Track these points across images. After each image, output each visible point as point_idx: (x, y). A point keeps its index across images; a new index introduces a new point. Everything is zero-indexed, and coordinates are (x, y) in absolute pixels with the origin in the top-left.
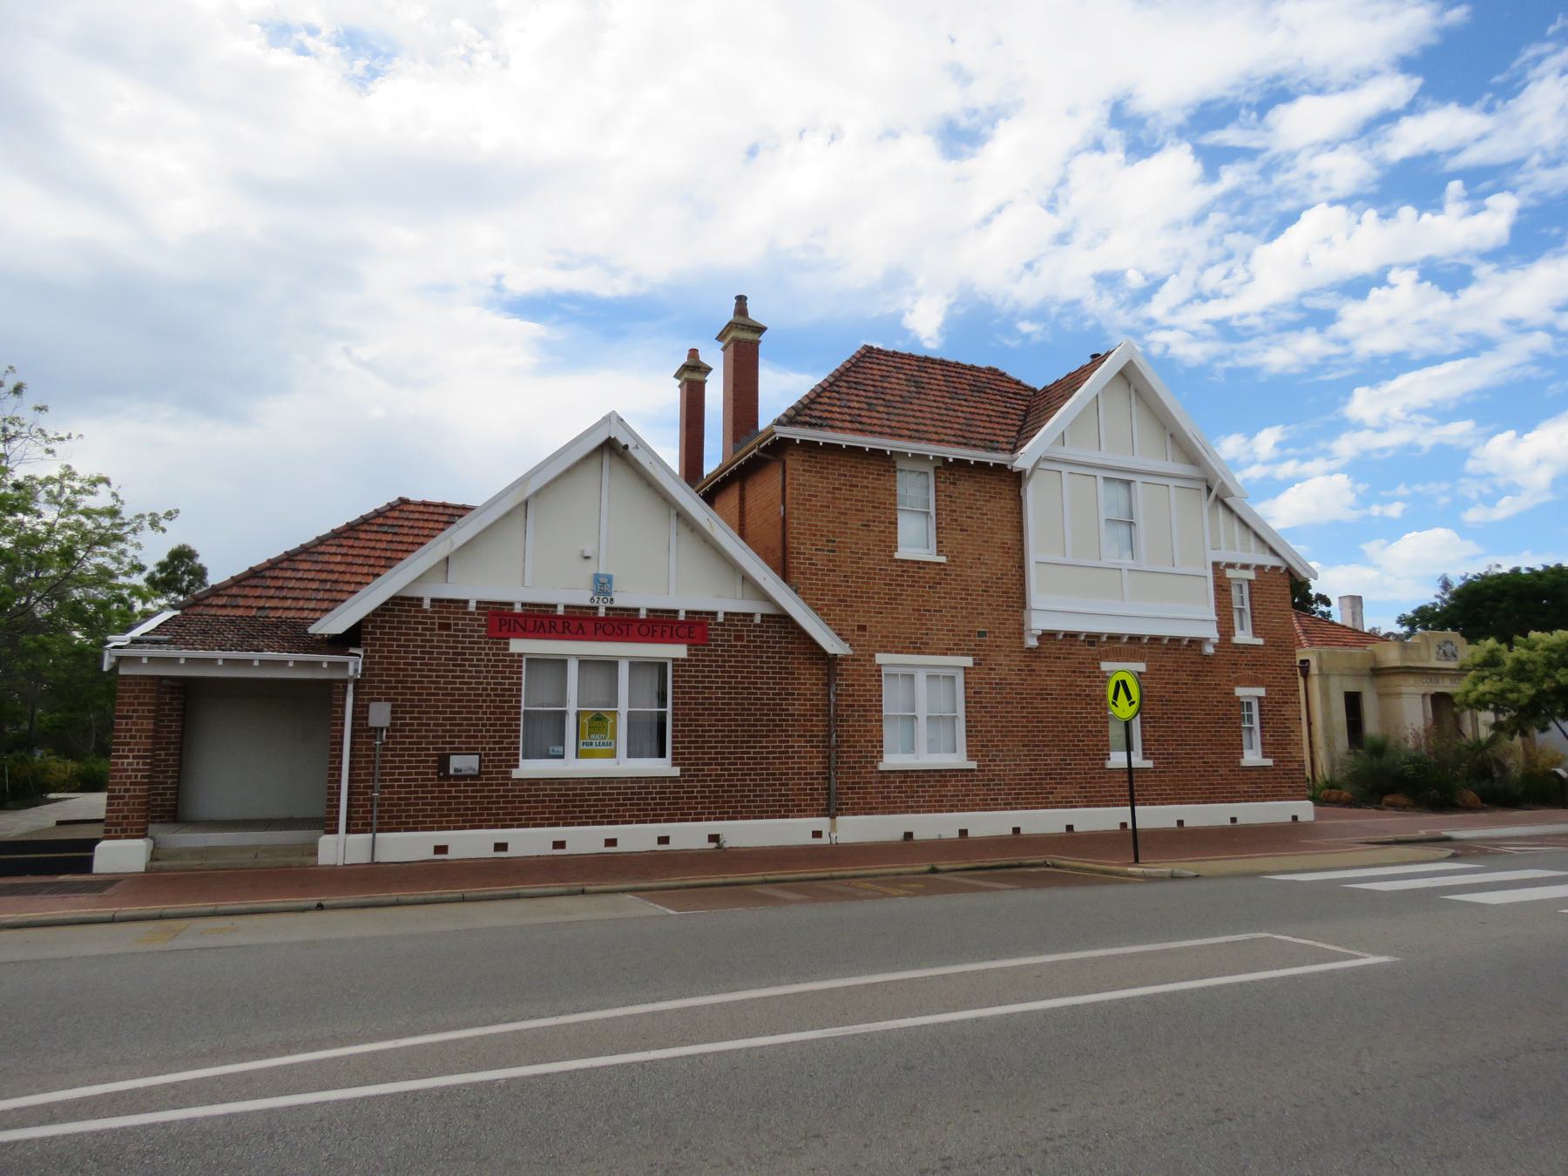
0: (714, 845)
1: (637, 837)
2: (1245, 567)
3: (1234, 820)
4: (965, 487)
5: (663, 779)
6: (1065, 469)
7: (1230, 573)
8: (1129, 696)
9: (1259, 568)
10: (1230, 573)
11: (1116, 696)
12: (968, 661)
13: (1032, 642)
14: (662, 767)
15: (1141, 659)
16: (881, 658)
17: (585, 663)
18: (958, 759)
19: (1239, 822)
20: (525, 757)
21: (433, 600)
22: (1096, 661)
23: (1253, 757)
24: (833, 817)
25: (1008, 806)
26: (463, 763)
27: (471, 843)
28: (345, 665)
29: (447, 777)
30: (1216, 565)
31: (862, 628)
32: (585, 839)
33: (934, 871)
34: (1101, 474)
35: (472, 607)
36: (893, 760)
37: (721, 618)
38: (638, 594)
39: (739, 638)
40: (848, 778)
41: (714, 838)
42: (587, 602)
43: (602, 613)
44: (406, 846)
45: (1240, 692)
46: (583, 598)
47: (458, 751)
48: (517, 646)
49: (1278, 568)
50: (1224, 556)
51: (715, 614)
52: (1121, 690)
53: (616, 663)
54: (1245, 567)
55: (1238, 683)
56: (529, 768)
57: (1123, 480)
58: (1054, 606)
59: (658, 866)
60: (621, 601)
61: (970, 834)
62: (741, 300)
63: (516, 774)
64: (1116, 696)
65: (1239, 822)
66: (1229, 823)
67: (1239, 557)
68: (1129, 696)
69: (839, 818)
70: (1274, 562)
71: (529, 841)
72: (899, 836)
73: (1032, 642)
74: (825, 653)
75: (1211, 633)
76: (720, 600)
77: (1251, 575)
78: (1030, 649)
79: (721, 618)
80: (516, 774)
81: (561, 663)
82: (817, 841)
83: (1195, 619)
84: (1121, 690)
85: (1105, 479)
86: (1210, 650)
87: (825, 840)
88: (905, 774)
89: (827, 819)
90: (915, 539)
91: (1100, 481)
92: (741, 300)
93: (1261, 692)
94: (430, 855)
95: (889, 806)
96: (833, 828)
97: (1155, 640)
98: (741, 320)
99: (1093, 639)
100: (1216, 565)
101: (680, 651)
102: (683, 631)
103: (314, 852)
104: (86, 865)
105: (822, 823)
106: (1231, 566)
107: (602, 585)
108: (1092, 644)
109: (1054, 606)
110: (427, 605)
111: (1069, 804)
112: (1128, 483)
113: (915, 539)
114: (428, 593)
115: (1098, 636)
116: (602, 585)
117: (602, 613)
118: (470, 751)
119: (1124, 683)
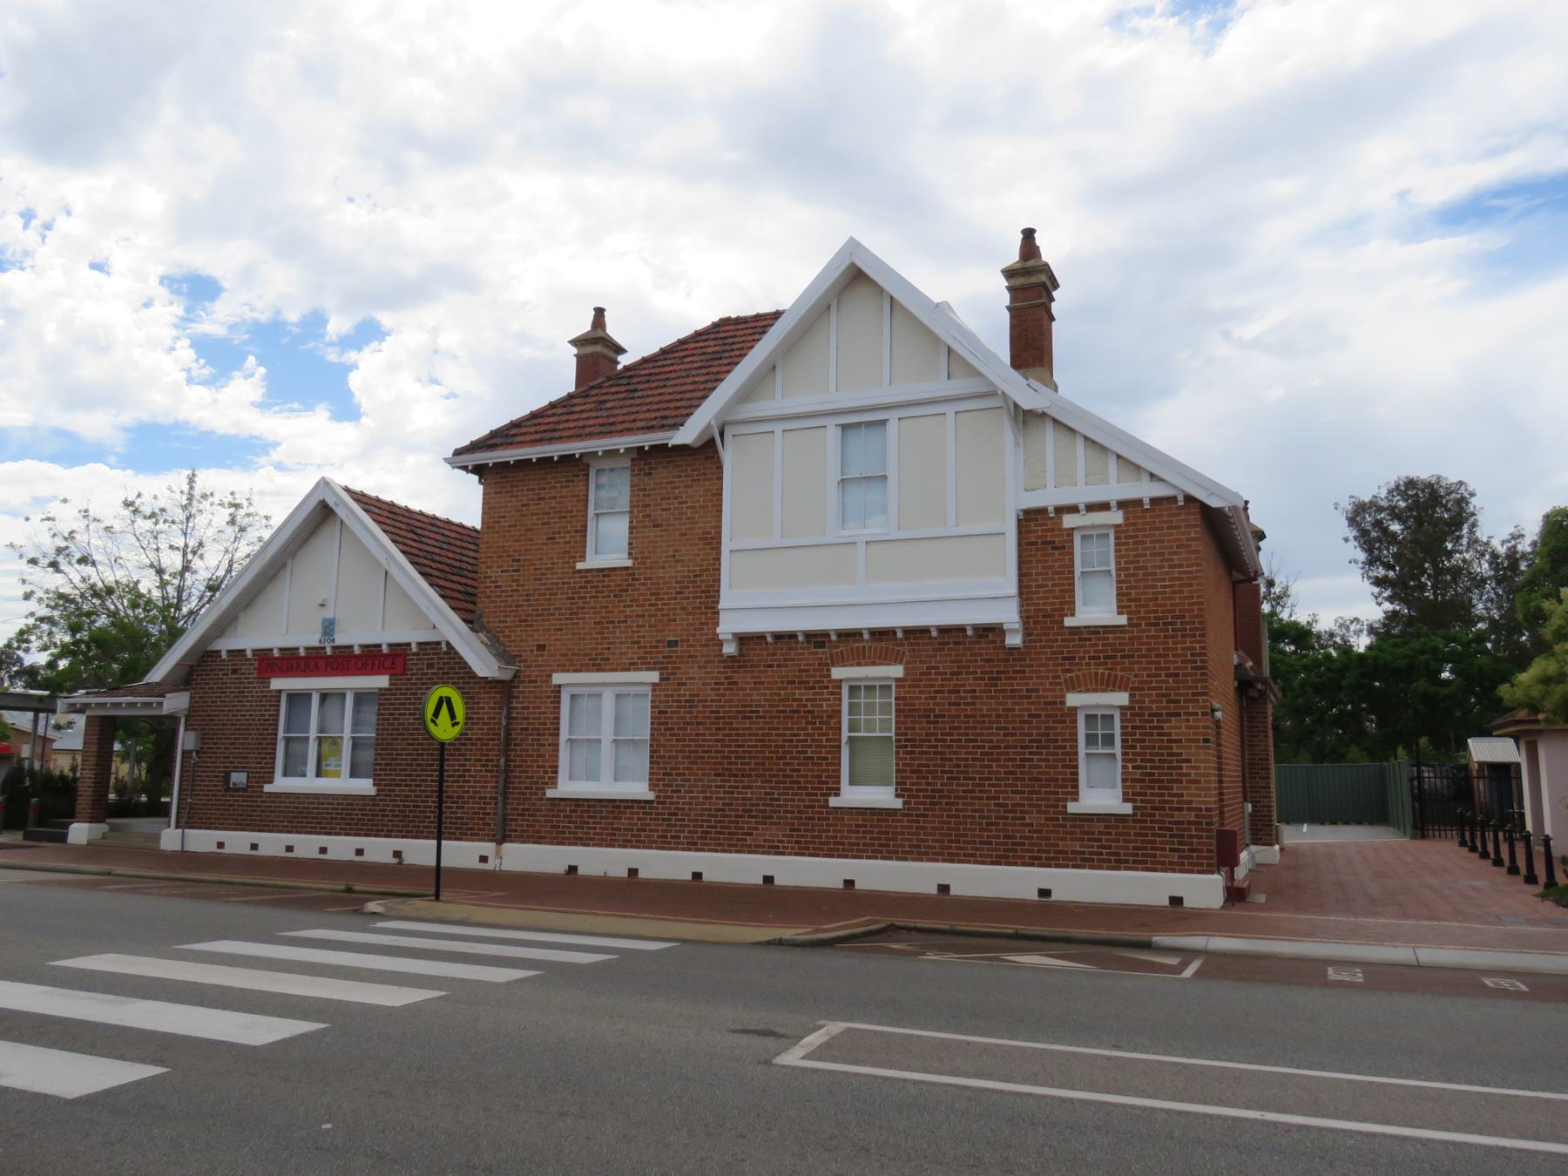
0: (395, 861)
1: (341, 847)
2: (1104, 507)
4: (662, 475)
5: (364, 797)
6: (778, 428)
7: (1069, 521)
8: (452, 716)
9: (1122, 505)
10: (1069, 521)
11: (437, 713)
12: (654, 676)
13: (730, 649)
14: (365, 786)
15: (897, 660)
16: (558, 678)
17: (324, 696)
18: (638, 788)
19: (1055, 897)
20: (285, 774)
21: (230, 652)
22: (825, 667)
24: (500, 842)
25: (692, 846)
26: (238, 778)
27: (238, 842)
28: (160, 704)
29: (228, 789)
30: (1030, 520)
31: (541, 647)
32: (306, 845)
33: (349, 890)
34: (831, 423)
35: (249, 654)
36: (567, 787)
37: (414, 648)
38: (353, 635)
39: (430, 666)
40: (523, 807)
41: (397, 854)
42: (316, 644)
43: (329, 651)
44: (202, 840)
46: (314, 641)
47: (236, 769)
48: (277, 684)
49: (1174, 499)
51: (409, 644)
53: (344, 695)
54: (1104, 507)
55: (1074, 686)
56: (282, 784)
57: (861, 424)
58: (750, 603)
59: (632, 894)
60: (341, 640)
61: (641, 875)
62: (600, 312)
63: (268, 788)
64: (437, 713)
65: (1055, 897)
66: (1034, 896)
67: (1081, 494)
68: (452, 716)
69: (507, 846)
70: (1159, 491)
71: (272, 844)
72: (561, 868)
73: (730, 649)
74: (473, 675)
75: (1007, 614)
76: (411, 635)
77: (1116, 517)
78: (731, 657)
79: (414, 648)
81: (342, 695)
82: (483, 866)
83: (987, 595)
85: (845, 427)
86: (1014, 640)
87: (489, 866)
88: (577, 802)
89: (493, 845)
90: (609, 543)
91: (832, 434)
92: (600, 312)
93: (1122, 698)
94: (214, 849)
95: (558, 837)
96: (499, 856)
97: (916, 634)
98: (600, 333)
99: (817, 639)
100: (1030, 520)
101: (382, 681)
102: (388, 663)
103: (157, 838)
104: (63, 838)
105: (488, 848)
106: (1073, 509)
107: (329, 627)
108: (821, 645)
109: (750, 603)
110: (224, 655)
112: (883, 422)
113: (609, 543)
114: (224, 645)
115: (825, 634)
116: (329, 627)
117: (329, 651)
118: (243, 769)
119: (449, 700)
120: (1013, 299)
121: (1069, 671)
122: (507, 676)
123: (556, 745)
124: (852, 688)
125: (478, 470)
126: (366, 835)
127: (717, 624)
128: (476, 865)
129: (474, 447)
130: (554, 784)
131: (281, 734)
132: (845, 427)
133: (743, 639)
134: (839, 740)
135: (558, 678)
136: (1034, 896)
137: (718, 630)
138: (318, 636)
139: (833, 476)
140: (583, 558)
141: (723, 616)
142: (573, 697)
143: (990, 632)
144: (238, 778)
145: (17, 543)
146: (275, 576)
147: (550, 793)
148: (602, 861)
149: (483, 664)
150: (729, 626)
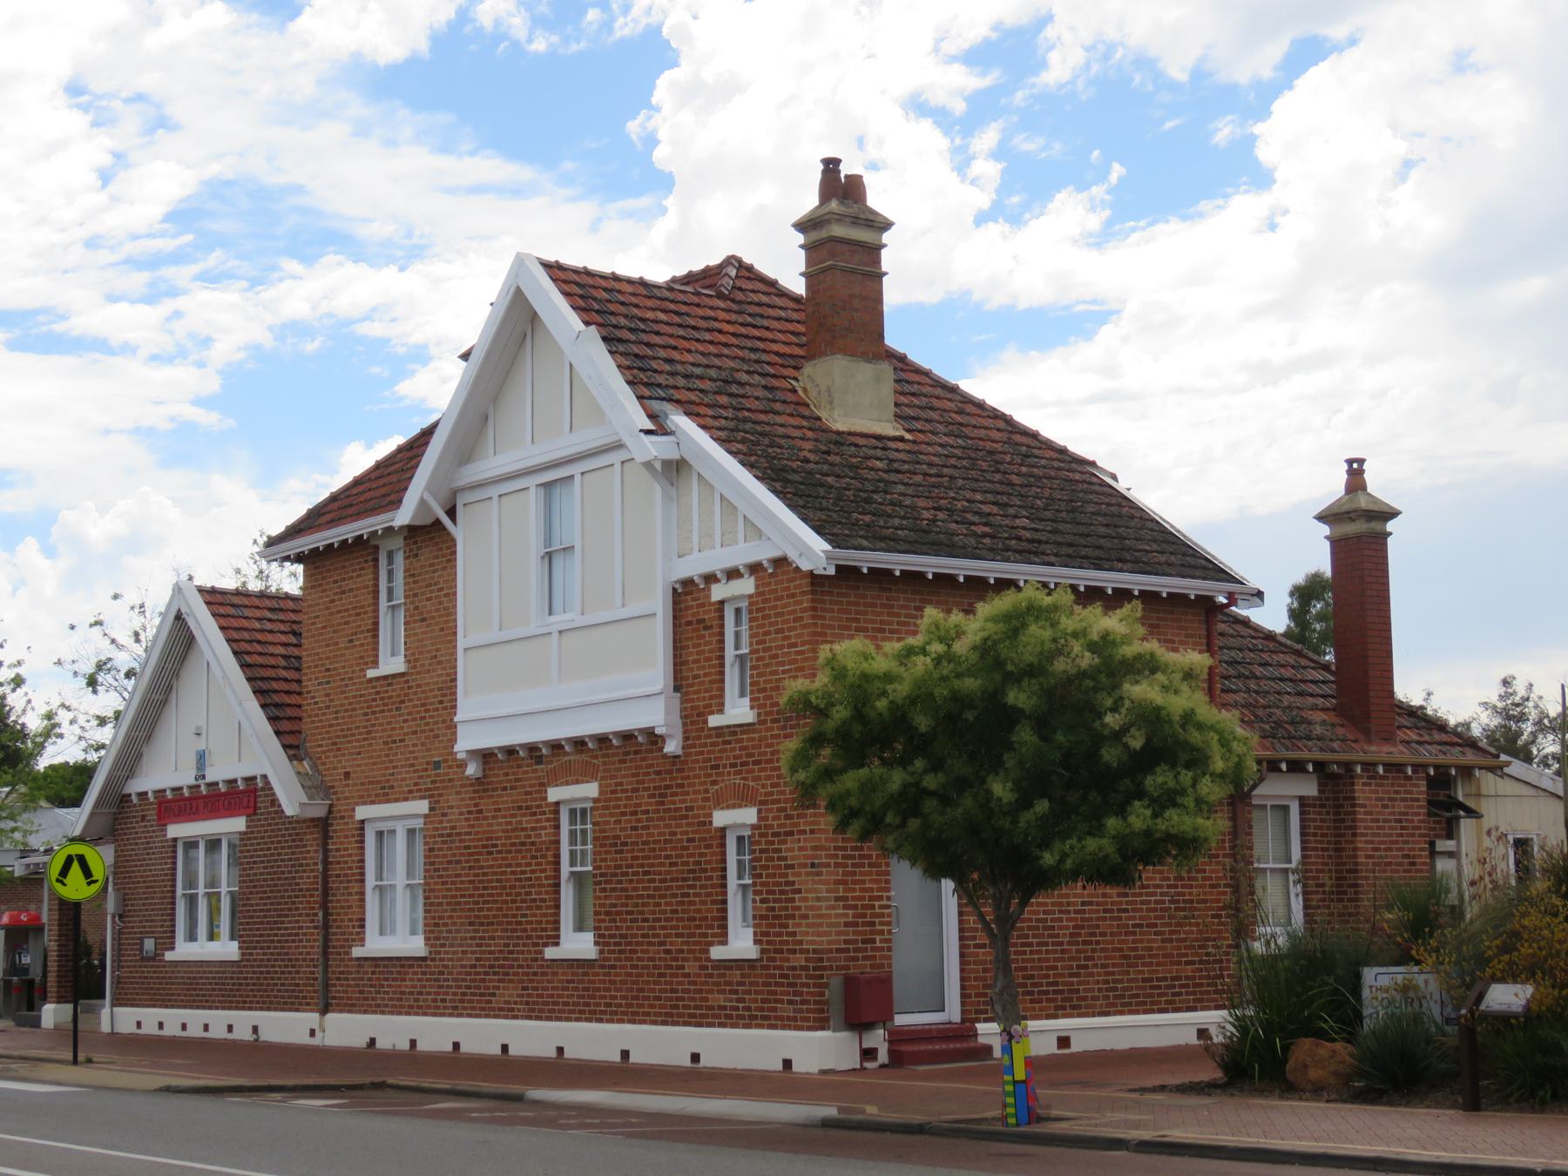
2: (733, 574)
3: (695, 1057)
6: (494, 491)
9: (755, 568)
10: (718, 592)
16: (362, 812)
23: (741, 943)
24: (324, 1011)
25: (455, 1012)
31: (347, 775)
45: (720, 818)
50: (693, 566)
52: (75, 865)
55: (722, 802)
56: (184, 950)
60: (212, 775)
65: (705, 1062)
66: (687, 1062)
80: (169, 956)
84: (75, 865)
86: (672, 747)
87: (316, 1041)
106: (710, 578)
110: (135, 799)
111: (509, 1012)
114: (135, 787)
117: (203, 790)
120: (809, 262)
121: (714, 783)
122: (320, 812)
123: (363, 893)
124: (573, 812)
125: (299, 558)
126: (549, 1019)
127: (454, 740)
128: (306, 1040)
129: (294, 531)
130: (361, 941)
131: (179, 891)
132: (547, 486)
133: (486, 756)
134: (558, 877)
135: (362, 812)
136: (687, 1062)
137: (456, 748)
138: (193, 773)
139: (535, 548)
140: (375, 664)
141: (460, 730)
142: (380, 834)
143: (654, 738)
144: (149, 944)
145: (67, 657)
146: (164, 702)
147: (357, 952)
148: (393, 1031)
149: (291, 798)
150: (468, 741)
